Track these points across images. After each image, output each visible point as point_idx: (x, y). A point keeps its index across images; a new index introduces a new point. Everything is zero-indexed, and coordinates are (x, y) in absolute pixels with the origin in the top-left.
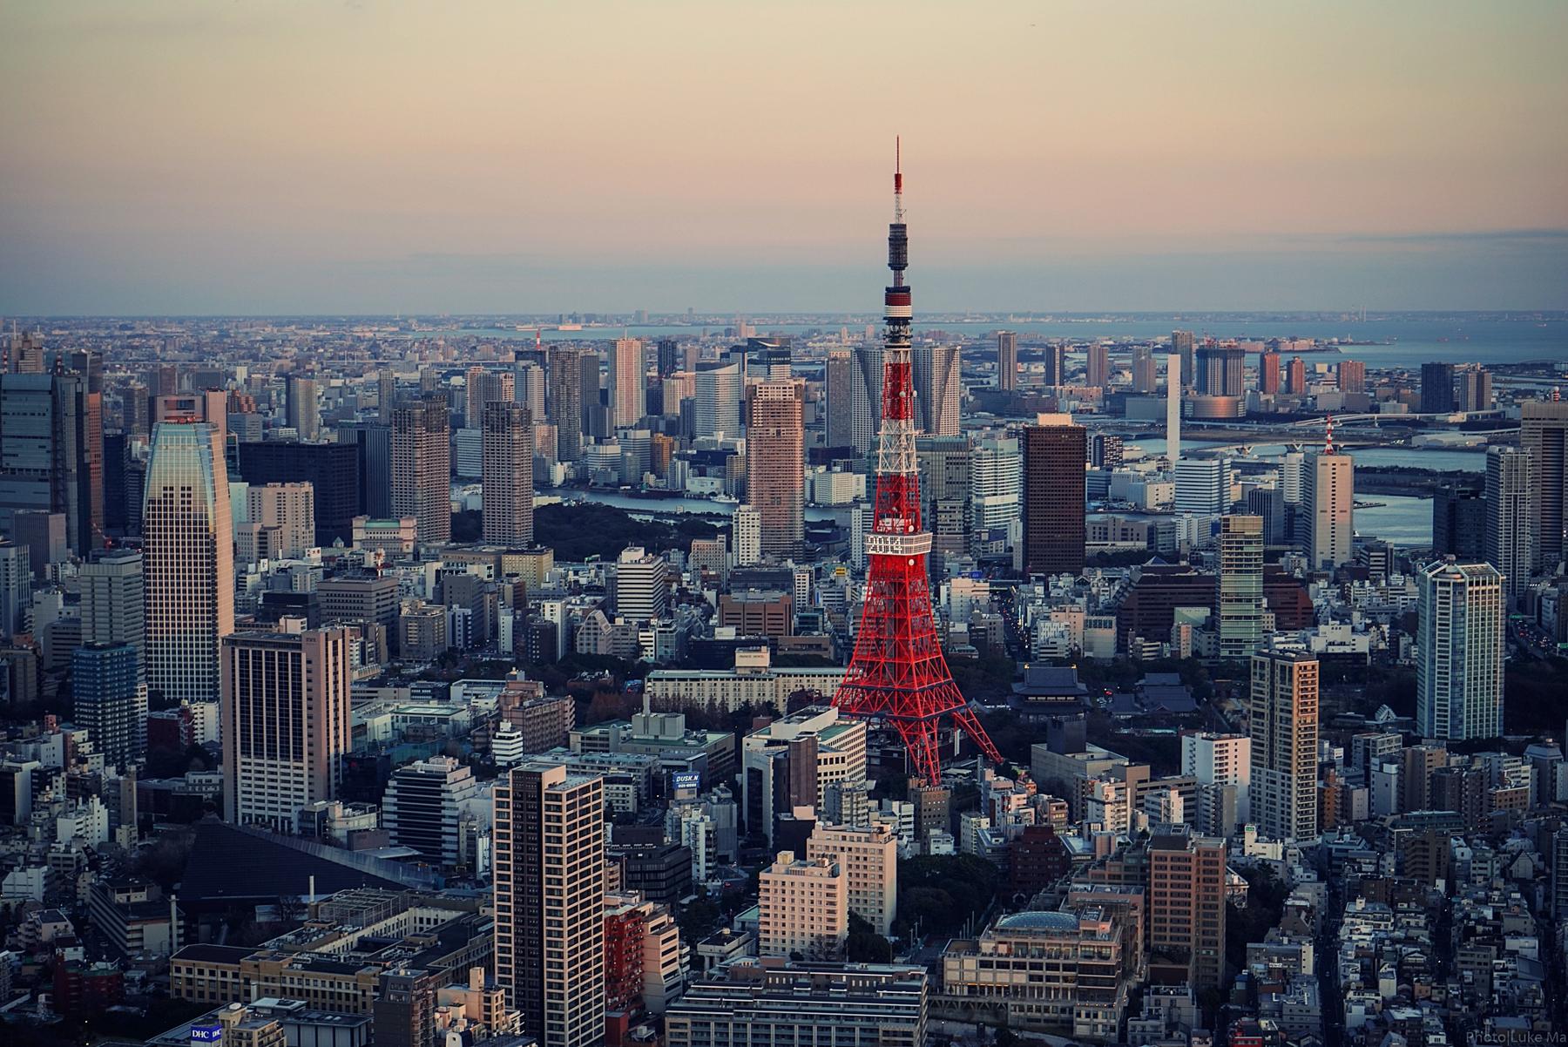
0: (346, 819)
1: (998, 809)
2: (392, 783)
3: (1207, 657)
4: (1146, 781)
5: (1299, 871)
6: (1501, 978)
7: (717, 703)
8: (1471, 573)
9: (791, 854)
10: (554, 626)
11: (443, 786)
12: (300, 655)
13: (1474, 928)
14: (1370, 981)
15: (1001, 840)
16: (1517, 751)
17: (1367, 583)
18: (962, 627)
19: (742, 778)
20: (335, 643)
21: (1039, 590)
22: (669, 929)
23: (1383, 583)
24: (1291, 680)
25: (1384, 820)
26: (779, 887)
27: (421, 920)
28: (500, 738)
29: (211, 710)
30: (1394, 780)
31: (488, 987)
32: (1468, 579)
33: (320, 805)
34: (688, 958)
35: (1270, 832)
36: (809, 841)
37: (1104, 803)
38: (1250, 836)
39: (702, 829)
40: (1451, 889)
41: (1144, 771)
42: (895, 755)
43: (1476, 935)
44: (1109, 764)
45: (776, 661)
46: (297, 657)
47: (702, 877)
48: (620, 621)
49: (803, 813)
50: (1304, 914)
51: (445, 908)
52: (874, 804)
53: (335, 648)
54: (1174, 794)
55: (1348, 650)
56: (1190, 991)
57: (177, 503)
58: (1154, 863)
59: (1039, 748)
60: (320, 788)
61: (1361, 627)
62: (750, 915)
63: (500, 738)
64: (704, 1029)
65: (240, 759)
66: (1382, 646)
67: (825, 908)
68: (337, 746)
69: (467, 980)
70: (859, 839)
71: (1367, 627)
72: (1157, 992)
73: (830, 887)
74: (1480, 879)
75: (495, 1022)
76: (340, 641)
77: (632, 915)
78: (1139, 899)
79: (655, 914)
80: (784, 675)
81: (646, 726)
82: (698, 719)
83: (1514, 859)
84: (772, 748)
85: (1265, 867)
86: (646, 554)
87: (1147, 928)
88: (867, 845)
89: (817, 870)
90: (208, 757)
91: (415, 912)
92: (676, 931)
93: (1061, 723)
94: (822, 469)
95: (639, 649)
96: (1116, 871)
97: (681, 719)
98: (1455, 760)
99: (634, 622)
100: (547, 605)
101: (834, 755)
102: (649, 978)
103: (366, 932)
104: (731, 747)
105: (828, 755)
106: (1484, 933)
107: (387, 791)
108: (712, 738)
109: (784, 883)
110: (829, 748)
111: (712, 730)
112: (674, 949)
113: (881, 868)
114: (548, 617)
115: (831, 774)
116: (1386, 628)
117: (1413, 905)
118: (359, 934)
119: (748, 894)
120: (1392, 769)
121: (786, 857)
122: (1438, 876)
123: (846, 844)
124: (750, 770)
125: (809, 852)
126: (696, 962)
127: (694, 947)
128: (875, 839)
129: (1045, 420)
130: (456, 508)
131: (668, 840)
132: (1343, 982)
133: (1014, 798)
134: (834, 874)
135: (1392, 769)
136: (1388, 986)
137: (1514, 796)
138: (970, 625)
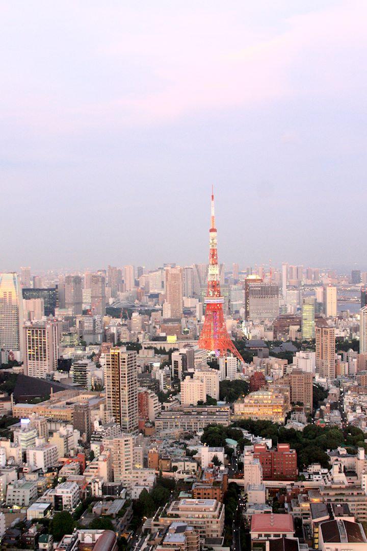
0: (58, 376)
1: (245, 371)
2: (72, 367)
5: (331, 386)
7: (163, 348)
10: (113, 334)
11: (87, 367)
14: (355, 411)
15: (248, 377)
18: (230, 332)
20: (55, 327)
22: (155, 397)
23: (347, 320)
29: (18, 352)
30: (356, 364)
31: (105, 409)
33: (52, 372)
34: (160, 406)
35: (322, 376)
39: (162, 375)
41: (286, 361)
46: (44, 331)
47: (162, 388)
48: (132, 332)
49: (190, 370)
50: (334, 395)
51: (90, 394)
53: (55, 329)
55: (339, 336)
57: (8, 296)
60: (52, 369)
61: (342, 331)
62: (177, 397)
64: (166, 424)
67: (200, 391)
68: (56, 357)
69: (99, 408)
71: (344, 330)
75: (107, 420)
77: (145, 392)
78: (289, 388)
79: (151, 393)
81: (143, 353)
82: (158, 352)
84: (181, 355)
87: (291, 397)
88: (211, 376)
89: (197, 381)
90: (18, 364)
92: (157, 398)
95: (138, 340)
96: (281, 381)
97: (153, 351)
99: (137, 332)
100: (112, 328)
101: (198, 357)
103: (68, 401)
104: (168, 359)
105: (197, 357)
107: (71, 369)
110: (197, 355)
112: (156, 403)
114: (112, 331)
116: (349, 331)
117: (364, 393)
118: (66, 401)
121: (188, 377)
124: (175, 361)
126: (163, 408)
127: (162, 404)
130: (83, 309)
131: (153, 377)
134: (202, 381)
135: (355, 360)
136: (359, 411)
138: (232, 332)
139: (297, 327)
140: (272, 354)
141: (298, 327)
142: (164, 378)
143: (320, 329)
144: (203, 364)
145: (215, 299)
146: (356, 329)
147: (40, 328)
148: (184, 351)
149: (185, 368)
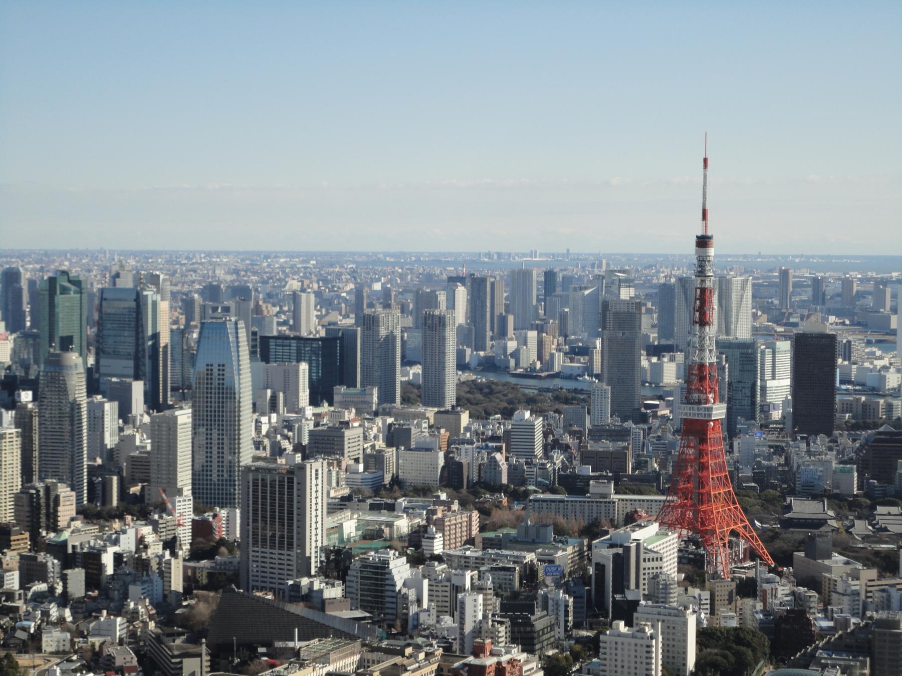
1: (769, 596)
4: (874, 580)
9: (622, 624)
20: (317, 471)
26: (614, 646)
36: (635, 615)
37: (843, 595)
41: (873, 573)
42: (698, 557)
44: (848, 568)
46: (291, 481)
49: (630, 596)
65: (251, 548)
80: (623, 500)
101: (655, 556)
105: (651, 555)
109: (616, 643)
115: (653, 568)
124: (597, 564)
125: (635, 621)
133: (780, 588)
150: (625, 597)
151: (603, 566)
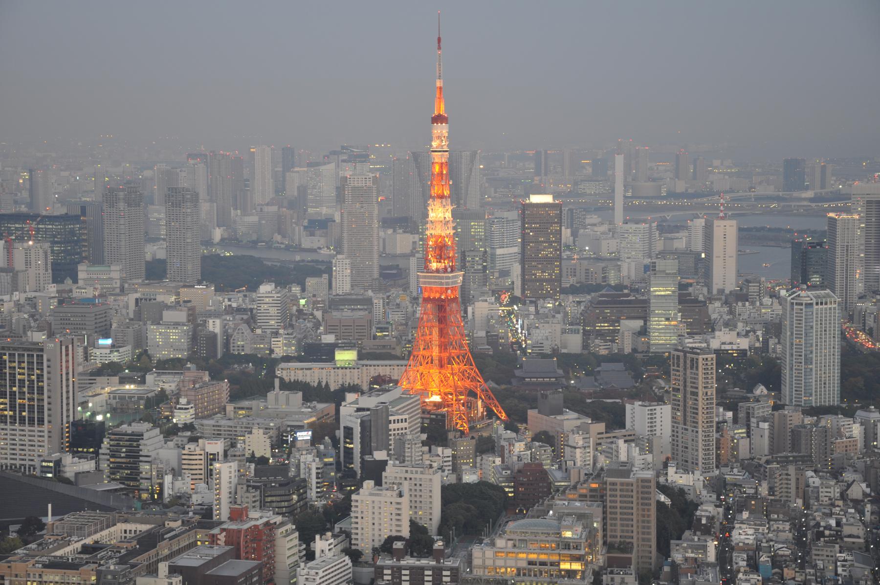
0: (73, 466)
1: (506, 452)
3: (642, 352)
4: (602, 433)
5: (704, 493)
6: (843, 566)
7: (324, 384)
8: (817, 297)
12: (42, 356)
13: (823, 532)
15: (509, 472)
16: (849, 413)
17: (747, 303)
18: (482, 334)
19: (340, 433)
20: (67, 347)
21: (532, 309)
23: (758, 304)
24: (697, 369)
25: (760, 459)
27: (125, 532)
28: (180, 409)
30: (767, 433)
32: (814, 301)
33: (56, 456)
34: (304, 552)
35: (686, 467)
36: (384, 473)
37: (575, 448)
38: (671, 470)
39: (314, 466)
40: (807, 506)
41: (601, 427)
42: (439, 417)
43: (824, 536)
44: (578, 423)
45: (361, 357)
47: (314, 498)
48: (259, 331)
49: (380, 455)
52: (426, 449)
53: (67, 350)
54: (621, 442)
56: (633, 573)
58: (609, 487)
59: (532, 413)
61: (744, 333)
63: (180, 409)
66: (757, 345)
68: (68, 416)
70: (416, 472)
72: (612, 573)
73: (398, 503)
74: (827, 499)
76: (70, 347)
77: (267, 524)
79: (282, 524)
80: (367, 366)
81: (277, 399)
83: (849, 486)
85: (682, 492)
86: (276, 287)
89: (389, 493)
91: (121, 526)
92: (297, 534)
93: (546, 396)
94: (390, 231)
96: (584, 491)
97: (300, 394)
98: (808, 420)
99: (268, 331)
100: (211, 321)
101: (400, 417)
102: (278, 566)
103: (89, 541)
104: (333, 412)
105: (396, 418)
106: (830, 536)
107: (102, 445)
108: (320, 406)
111: (320, 401)
113: (431, 491)
114: (211, 328)
115: (398, 429)
116: (759, 333)
117: (781, 516)
119: (343, 510)
120: (766, 426)
121: (369, 484)
122: (797, 496)
123: (408, 476)
125: (384, 480)
128: (427, 472)
129: (535, 199)
130: (148, 257)
132: (735, 566)
133: (517, 445)
134: (400, 495)
135: (766, 426)
137: (848, 444)
138: (487, 332)
139: (638, 324)
140: (576, 404)
141: (639, 323)
142: (317, 473)
143: (681, 354)
144: (409, 437)
145: (442, 278)
146: (774, 329)
147: (28, 350)
148: (370, 402)
149: (366, 449)
150: (373, 457)
151: (352, 429)
